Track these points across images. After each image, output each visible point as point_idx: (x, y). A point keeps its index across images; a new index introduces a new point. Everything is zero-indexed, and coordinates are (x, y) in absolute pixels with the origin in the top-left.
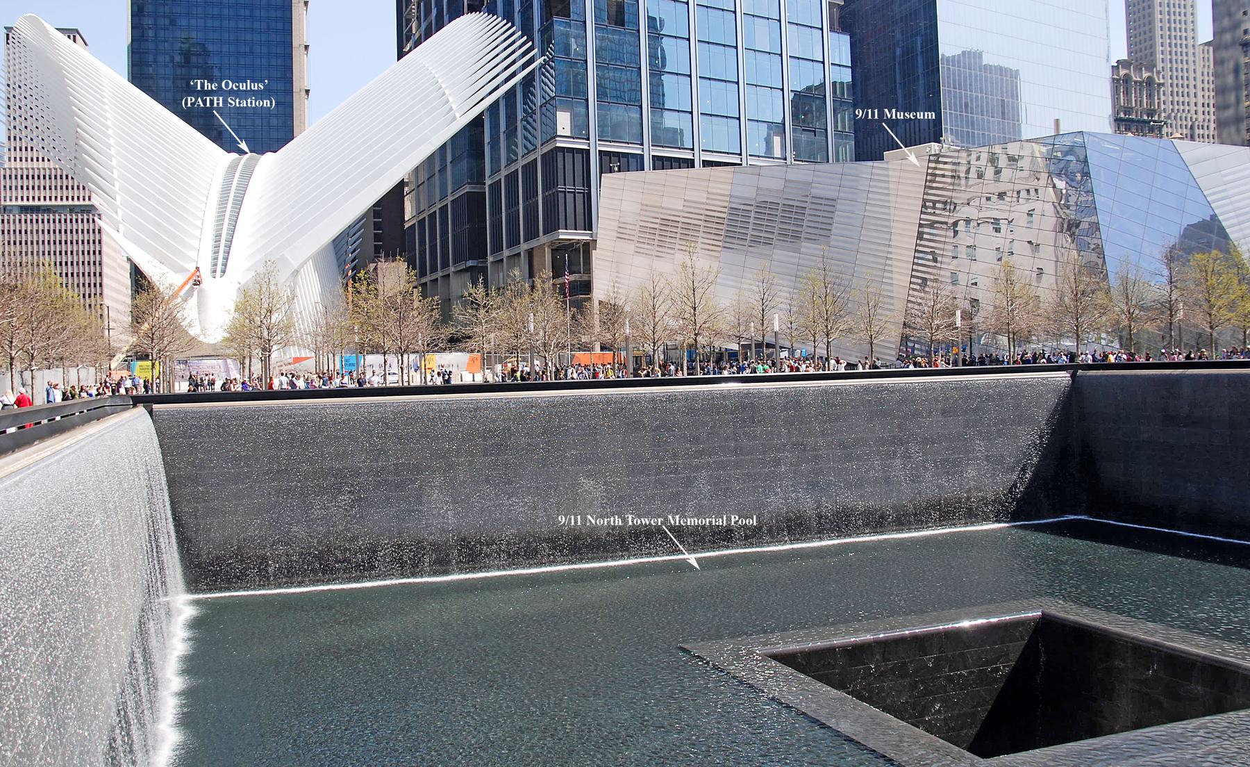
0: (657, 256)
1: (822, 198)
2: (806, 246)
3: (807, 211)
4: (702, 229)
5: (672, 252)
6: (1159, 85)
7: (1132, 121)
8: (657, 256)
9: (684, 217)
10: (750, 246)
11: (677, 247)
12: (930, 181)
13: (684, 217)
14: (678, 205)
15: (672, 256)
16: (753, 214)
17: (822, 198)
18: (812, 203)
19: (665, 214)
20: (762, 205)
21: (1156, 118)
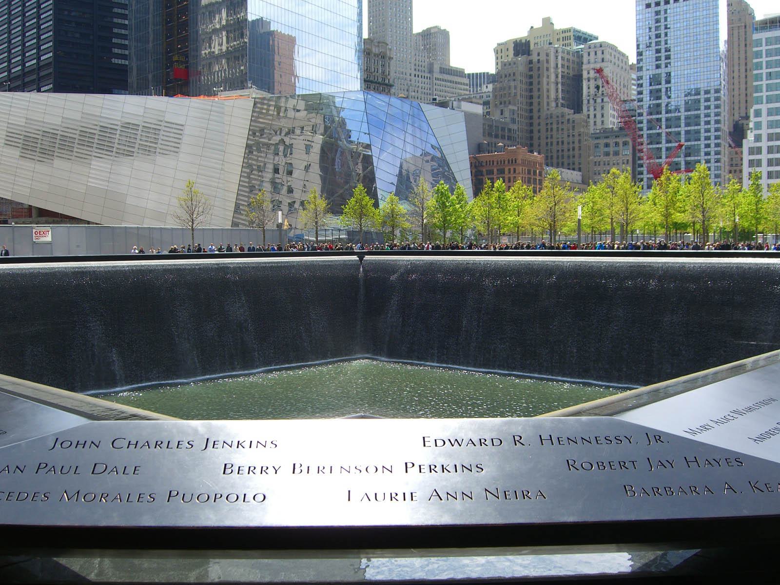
0: (39, 161)
1: (173, 124)
2: (160, 159)
3: (162, 133)
4: (76, 141)
5: (52, 158)
6: (391, 58)
7: (372, 82)
8: (39, 161)
9: (62, 131)
10: (116, 157)
11: (56, 154)
12: (256, 117)
13: (62, 131)
14: (58, 121)
15: (51, 161)
16: (118, 132)
17: (173, 124)
18: (165, 126)
19: (46, 127)
20: (126, 126)
21: (387, 81)
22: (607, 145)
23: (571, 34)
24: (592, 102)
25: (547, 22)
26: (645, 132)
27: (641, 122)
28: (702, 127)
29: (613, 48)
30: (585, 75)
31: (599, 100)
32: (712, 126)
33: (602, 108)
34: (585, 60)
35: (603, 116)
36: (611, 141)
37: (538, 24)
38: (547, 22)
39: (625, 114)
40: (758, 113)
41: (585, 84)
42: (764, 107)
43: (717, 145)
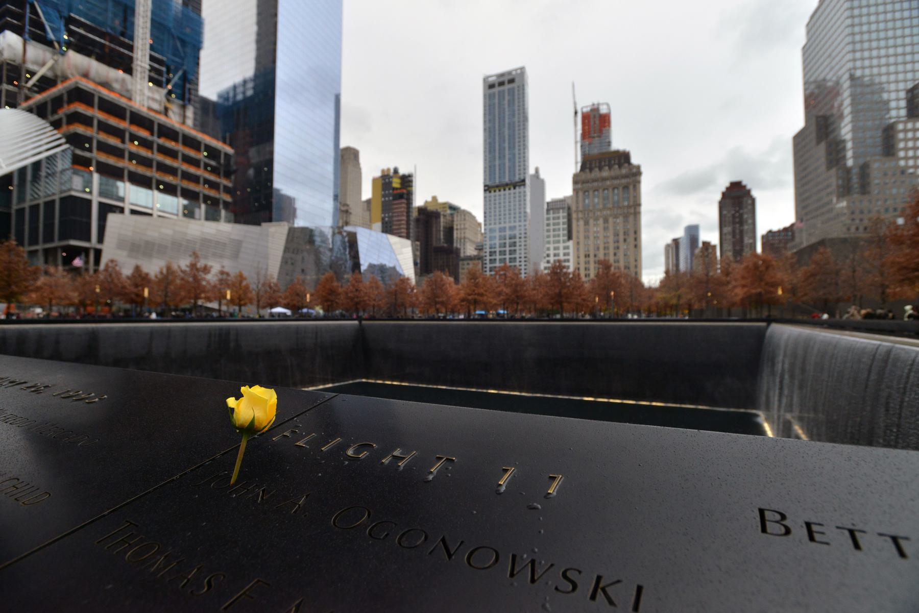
22: (468, 264)
23: (447, 206)
24: (459, 241)
25: (435, 198)
26: (488, 258)
27: (486, 252)
28: (517, 256)
29: (470, 214)
30: (455, 227)
31: (462, 241)
32: (523, 256)
33: (464, 245)
34: (455, 219)
35: (464, 249)
36: (471, 262)
37: (429, 199)
38: (435, 198)
39: (477, 248)
40: (548, 249)
41: (455, 232)
42: (552, 246)
43: (525, 265)
